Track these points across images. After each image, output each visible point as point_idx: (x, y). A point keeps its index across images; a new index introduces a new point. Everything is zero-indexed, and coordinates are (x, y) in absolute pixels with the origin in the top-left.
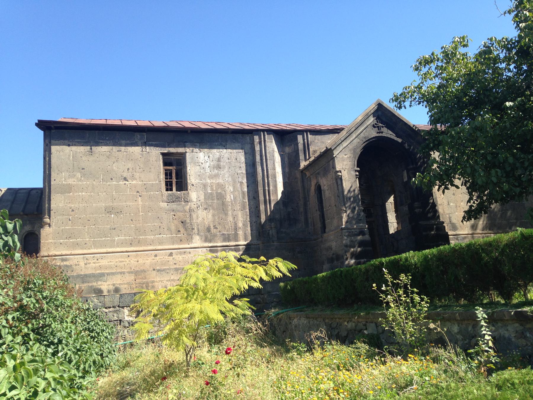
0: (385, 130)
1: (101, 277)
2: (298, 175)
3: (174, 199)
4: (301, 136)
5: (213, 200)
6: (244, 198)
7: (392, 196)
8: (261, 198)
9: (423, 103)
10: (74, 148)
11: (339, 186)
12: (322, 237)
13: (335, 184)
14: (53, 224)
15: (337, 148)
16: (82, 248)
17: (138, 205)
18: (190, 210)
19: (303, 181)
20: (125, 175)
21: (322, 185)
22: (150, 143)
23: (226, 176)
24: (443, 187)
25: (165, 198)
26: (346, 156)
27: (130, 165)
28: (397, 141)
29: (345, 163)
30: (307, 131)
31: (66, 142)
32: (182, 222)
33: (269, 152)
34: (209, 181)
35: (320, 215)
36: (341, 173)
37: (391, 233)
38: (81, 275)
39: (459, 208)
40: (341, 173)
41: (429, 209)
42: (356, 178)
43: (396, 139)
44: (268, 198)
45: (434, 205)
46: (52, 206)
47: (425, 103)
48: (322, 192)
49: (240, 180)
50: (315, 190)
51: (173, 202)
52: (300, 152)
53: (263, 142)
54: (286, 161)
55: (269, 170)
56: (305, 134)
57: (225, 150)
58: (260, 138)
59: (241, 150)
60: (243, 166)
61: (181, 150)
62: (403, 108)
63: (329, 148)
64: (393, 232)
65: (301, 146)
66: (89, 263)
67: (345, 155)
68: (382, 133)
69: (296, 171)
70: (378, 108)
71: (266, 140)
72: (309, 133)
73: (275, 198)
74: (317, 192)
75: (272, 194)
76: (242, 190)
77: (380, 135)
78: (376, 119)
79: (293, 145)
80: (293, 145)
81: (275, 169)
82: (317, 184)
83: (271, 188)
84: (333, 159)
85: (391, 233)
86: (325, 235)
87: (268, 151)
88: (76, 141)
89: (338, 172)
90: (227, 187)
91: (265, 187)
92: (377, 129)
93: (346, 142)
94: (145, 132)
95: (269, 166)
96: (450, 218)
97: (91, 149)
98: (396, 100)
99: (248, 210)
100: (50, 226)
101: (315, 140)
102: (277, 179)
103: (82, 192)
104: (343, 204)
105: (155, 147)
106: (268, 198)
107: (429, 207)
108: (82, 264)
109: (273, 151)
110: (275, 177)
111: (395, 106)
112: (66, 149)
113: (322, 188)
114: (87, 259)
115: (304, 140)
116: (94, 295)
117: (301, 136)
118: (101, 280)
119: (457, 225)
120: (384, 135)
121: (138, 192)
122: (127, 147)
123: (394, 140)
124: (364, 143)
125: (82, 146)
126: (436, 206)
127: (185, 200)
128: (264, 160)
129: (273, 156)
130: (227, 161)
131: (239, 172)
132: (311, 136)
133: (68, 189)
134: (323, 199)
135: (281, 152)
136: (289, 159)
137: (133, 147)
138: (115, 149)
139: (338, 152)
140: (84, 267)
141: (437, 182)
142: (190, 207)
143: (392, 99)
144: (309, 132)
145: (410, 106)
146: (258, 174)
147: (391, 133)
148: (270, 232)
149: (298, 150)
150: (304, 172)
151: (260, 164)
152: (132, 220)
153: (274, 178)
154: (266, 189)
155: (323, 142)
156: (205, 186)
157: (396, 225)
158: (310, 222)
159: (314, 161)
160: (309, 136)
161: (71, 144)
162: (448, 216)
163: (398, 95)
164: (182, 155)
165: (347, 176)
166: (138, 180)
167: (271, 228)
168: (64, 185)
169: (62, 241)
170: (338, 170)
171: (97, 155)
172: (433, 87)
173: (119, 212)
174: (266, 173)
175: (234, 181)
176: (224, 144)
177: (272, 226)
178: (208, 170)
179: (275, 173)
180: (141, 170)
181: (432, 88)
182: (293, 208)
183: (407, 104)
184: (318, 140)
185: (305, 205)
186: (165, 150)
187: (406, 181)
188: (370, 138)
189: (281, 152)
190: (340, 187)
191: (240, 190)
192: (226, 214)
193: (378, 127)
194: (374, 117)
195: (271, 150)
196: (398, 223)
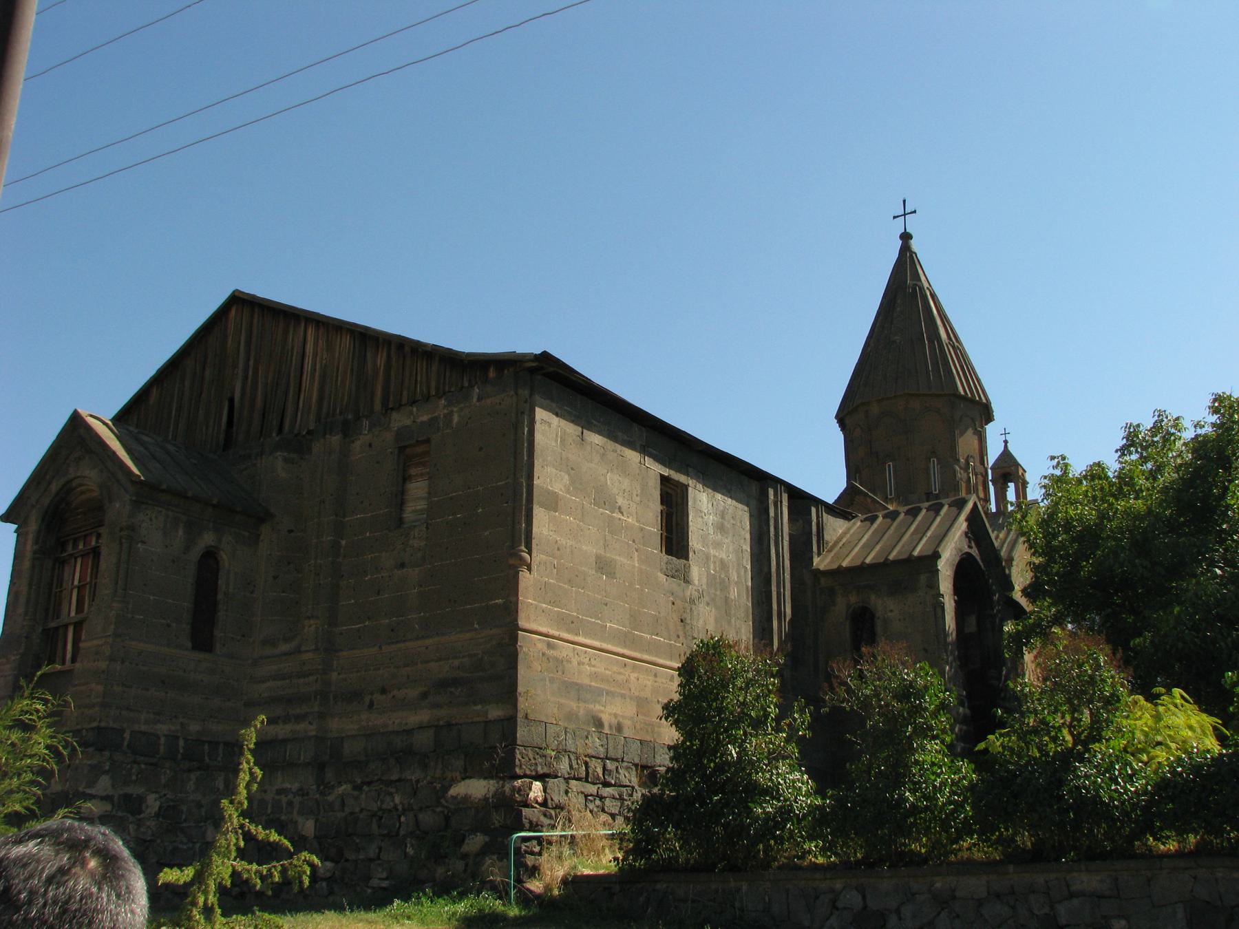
0: (973, 545)
1: (599, 695)
3: (674, 572)
5: (716, 590)
6: (748, 598)
8: (775, 606)
10: (563, 423)
14: (534, 567)
16: (569, 631)
17: (634, 567)
18: (692, 602)
20: (620, 501)
22: (650, 450)
23: (731, 549)
25: (664, 567)
27: (626, 483)
28: (980, 567)
31: (554, 405)
32: (682, 621)
34: (712, 552)
38: (577, 684)
43: (981, 564)
46: (535, 530)
49: (745, 563)
51: (672, 577)
57: (730, 500)
58: (776, 495)
59: (746, 508)
60: (748, 536)
61: (682, 478)
66: (583, 664)
69: (804, 570)
71: (783, 501)
76: (746, 583)
79: (801, 521)
80: (801, 521)
88: (565, 410)
90: (731, 571)
91: (780, 589)
94: (645, 427)
97: (582, 433)
99: (751, 623)
100: (529, 569)
103: (570, 514)
105: (654, 460)
108: (575, 663)
112: (555, 420)
114: (578, 654)
116: (594, 729)
118: (599, 702)
121: (634, 541)
122: (624, 448)
125: (572, 422)
127: (686, 576)
130: (732, 521)
131: (744, 547)
133: (553, 503)
137: (630, 451)
138: (610, 445)
140: (576, 670)
142: (691, 595)
147: (977, 552)
152: (626, 594)
154: (781, 592)
155: (834, 530)
156: (707, 557)
161: (557, 410)
164: (675, 488)
165: (948, 606)
166: (635, 516)
168: (548, 492)
169: (544, 605)
170: (941, 593)
171: (588, 448)
173: (611, 575)
175: (738, 565)
176: (729, 487)
178: (711, 531)
180: (638, 499)
184: (830, 525)
186: (666, 472)
191: (743, 581)
192: (729, 622)
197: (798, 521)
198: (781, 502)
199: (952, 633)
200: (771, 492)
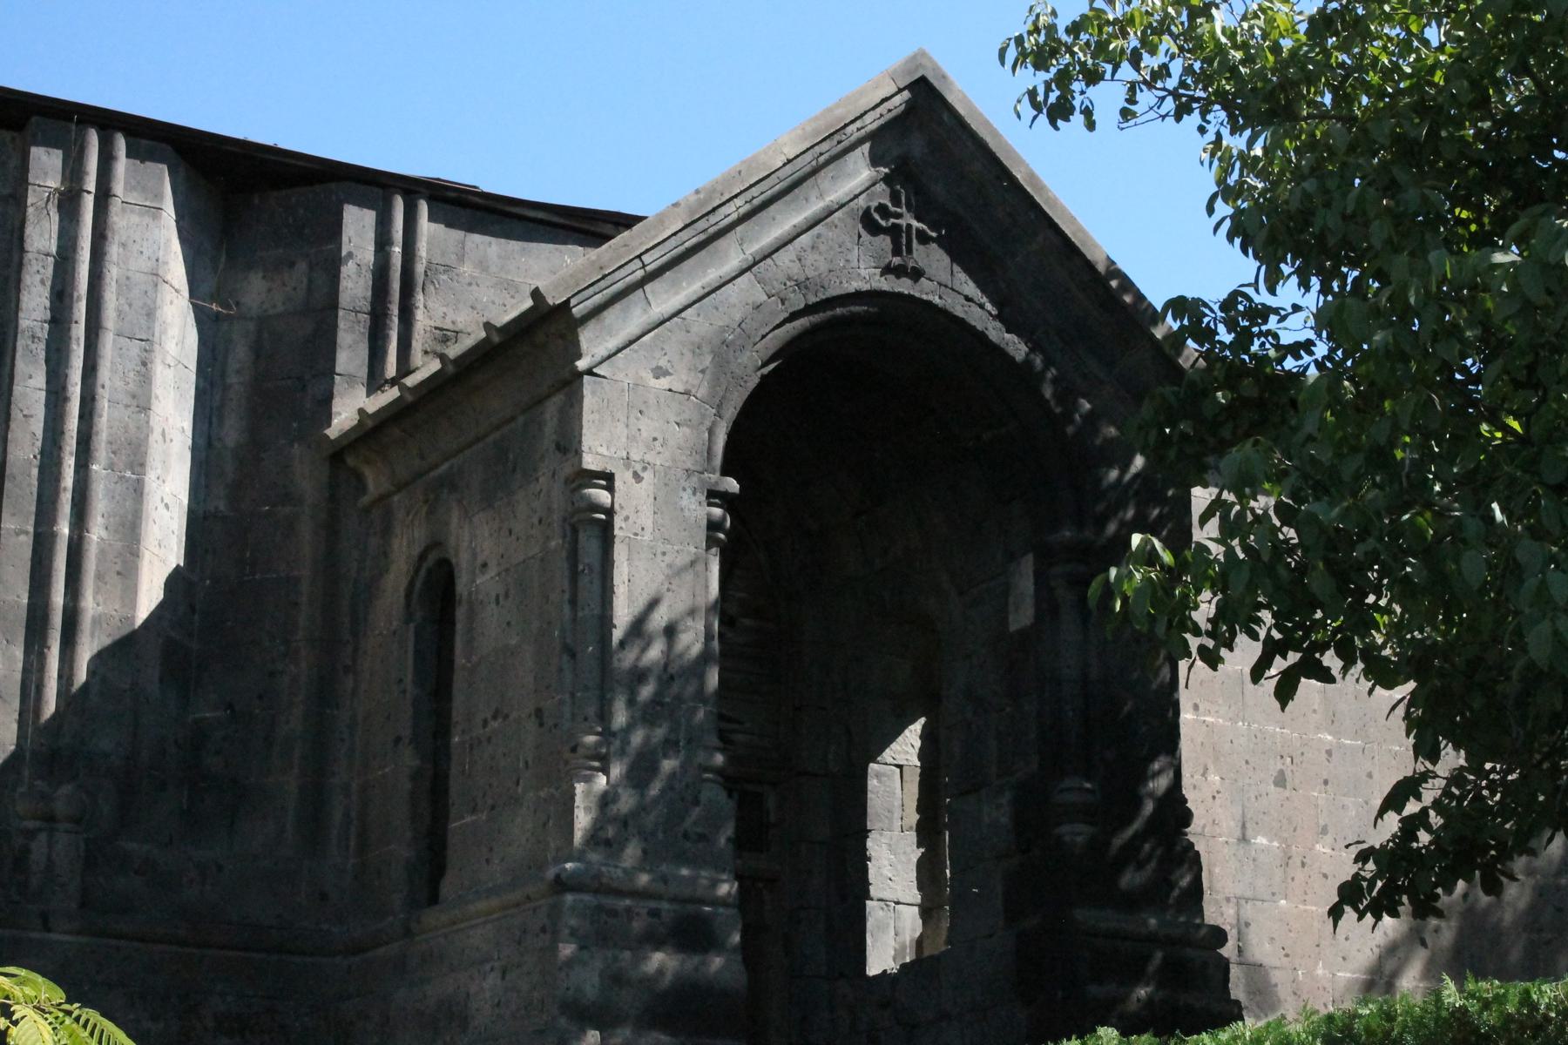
0: (933, 259)
2: (307, 479)
4: (369, 217)
7: (917, 727)
9: (1204, 112)
11: (584, 581)
12: (408, 933)
13: (561, 565)
15: (610, 315)
19: (331, 528)
21: (462, 561)
24: (1293, 657)
26: (664, 383)
28: (997, 351)
29: (648, 427)
30: (413, 188)
33: (125, 284)
35: (415, 777)
36: (610, 488)
37: (873, 970)
39: (1300, 875)
40: (610, 488)
41: (1139, 838)
42: (711, 542)
43: (996, 332)
44: (58, 598)
45: (1175, 811)
47: (1218, 115)
48: (461, 613)
50: (408, 595)
52: (342, 324)
53: (89, 202)
54: (233, 365)
55: (104, 406)
56: (399, 205)
58: (73, 171)
62: (1078, 119)
63: (554, 299)
64: (892, 966)
65: (354, 285)
67: (659, 373)
68: (917, 274)
69: (297, 449)
70: (910, 107)
71: (118, 187)
72: (423, 208)
73: (113, 608)
74: (419, 615)
75: (99, 577)
77: (904, 286)
78: (887, 179)
79: (302, 266)
80: (302, 266)
81: (145, 408)
82: (432, 558)
83: (97, 532)
84: (571, 383)
85: (873, 970)
86: (432, 917)
87: (112, 273)
89: (591, 477)
91: (53, 521)
92: (885, 242)
93: (676, 285)
95: (104, 374)
96: (1243, 926)
98: (1041, 59)
101: (461, 258)
102: (151, 478)
104: (591, 711)
106: (58, 598)
107: (1137, 825)
109: (156, 277)
110: (135, 457)
111: (1032, 94)
113: (461, 587)
115: (382, 242)
117: (369, 217)
119: (1276, 977)
120: (925, 290)
123: (981, 337)
124: (794, 316)
126: (1186, 817)
128: (79, 331)
129: (150, 314)
132: (439, 228)
134: (460, 660)
135: (212, 299)
136: (257, 350)
139: (612, 344)
141: (1266, 616)
143: (1019, 41)
144: (431, 200)
145: (1126, 114)
146: (16, 414)
147: (971, 289)
148: (39, 848)
149: (333, 305)
150: (351, 461)
151: (40, 349)
153: (131, 467)
154: (53, 536)
157: (910, 922)
158: (338, 816)
159: (434, 385)
160: (426, 227)
162: (1230, 911)
163: (1062, 24)
165: (646, 519)
167: (50, 818)
170: (590, 462)
172: (1281, 21)
174: (72, 424)
177: (60, 808)
179: (144, 430)
181: (1270, 21)
182: (230, 706)
183: (1106, 97)
184: (482, 265)
185: (324, 695)
187: (1022, 632)
188: (834, 291)
189: (213, 298)
190: (589, 587)
193: (894, 231)
194: (875, 161)
195: (139, 264)
196: (926, 912)
197: (292, 265)
198: (104, 195)
199: (670, 631)
200: (46, 167)
